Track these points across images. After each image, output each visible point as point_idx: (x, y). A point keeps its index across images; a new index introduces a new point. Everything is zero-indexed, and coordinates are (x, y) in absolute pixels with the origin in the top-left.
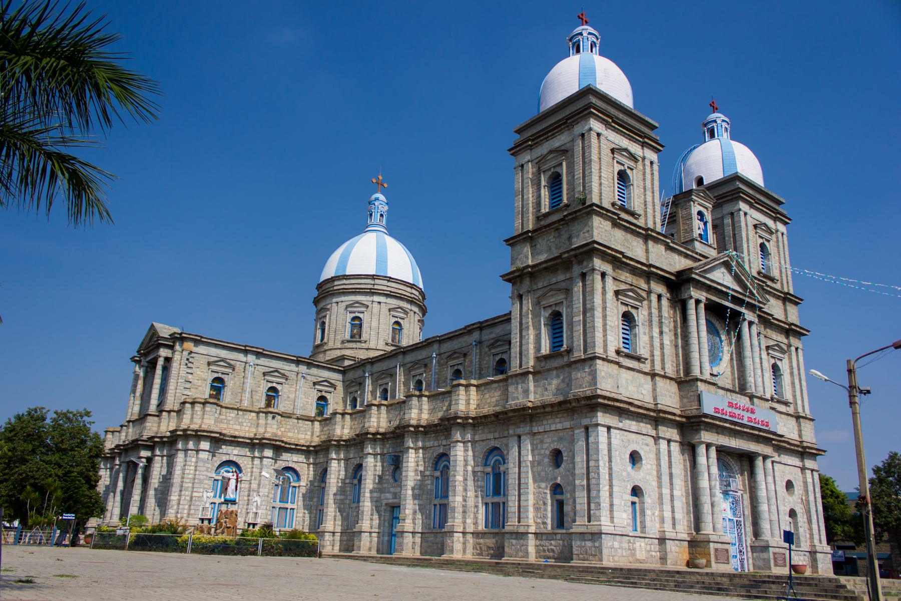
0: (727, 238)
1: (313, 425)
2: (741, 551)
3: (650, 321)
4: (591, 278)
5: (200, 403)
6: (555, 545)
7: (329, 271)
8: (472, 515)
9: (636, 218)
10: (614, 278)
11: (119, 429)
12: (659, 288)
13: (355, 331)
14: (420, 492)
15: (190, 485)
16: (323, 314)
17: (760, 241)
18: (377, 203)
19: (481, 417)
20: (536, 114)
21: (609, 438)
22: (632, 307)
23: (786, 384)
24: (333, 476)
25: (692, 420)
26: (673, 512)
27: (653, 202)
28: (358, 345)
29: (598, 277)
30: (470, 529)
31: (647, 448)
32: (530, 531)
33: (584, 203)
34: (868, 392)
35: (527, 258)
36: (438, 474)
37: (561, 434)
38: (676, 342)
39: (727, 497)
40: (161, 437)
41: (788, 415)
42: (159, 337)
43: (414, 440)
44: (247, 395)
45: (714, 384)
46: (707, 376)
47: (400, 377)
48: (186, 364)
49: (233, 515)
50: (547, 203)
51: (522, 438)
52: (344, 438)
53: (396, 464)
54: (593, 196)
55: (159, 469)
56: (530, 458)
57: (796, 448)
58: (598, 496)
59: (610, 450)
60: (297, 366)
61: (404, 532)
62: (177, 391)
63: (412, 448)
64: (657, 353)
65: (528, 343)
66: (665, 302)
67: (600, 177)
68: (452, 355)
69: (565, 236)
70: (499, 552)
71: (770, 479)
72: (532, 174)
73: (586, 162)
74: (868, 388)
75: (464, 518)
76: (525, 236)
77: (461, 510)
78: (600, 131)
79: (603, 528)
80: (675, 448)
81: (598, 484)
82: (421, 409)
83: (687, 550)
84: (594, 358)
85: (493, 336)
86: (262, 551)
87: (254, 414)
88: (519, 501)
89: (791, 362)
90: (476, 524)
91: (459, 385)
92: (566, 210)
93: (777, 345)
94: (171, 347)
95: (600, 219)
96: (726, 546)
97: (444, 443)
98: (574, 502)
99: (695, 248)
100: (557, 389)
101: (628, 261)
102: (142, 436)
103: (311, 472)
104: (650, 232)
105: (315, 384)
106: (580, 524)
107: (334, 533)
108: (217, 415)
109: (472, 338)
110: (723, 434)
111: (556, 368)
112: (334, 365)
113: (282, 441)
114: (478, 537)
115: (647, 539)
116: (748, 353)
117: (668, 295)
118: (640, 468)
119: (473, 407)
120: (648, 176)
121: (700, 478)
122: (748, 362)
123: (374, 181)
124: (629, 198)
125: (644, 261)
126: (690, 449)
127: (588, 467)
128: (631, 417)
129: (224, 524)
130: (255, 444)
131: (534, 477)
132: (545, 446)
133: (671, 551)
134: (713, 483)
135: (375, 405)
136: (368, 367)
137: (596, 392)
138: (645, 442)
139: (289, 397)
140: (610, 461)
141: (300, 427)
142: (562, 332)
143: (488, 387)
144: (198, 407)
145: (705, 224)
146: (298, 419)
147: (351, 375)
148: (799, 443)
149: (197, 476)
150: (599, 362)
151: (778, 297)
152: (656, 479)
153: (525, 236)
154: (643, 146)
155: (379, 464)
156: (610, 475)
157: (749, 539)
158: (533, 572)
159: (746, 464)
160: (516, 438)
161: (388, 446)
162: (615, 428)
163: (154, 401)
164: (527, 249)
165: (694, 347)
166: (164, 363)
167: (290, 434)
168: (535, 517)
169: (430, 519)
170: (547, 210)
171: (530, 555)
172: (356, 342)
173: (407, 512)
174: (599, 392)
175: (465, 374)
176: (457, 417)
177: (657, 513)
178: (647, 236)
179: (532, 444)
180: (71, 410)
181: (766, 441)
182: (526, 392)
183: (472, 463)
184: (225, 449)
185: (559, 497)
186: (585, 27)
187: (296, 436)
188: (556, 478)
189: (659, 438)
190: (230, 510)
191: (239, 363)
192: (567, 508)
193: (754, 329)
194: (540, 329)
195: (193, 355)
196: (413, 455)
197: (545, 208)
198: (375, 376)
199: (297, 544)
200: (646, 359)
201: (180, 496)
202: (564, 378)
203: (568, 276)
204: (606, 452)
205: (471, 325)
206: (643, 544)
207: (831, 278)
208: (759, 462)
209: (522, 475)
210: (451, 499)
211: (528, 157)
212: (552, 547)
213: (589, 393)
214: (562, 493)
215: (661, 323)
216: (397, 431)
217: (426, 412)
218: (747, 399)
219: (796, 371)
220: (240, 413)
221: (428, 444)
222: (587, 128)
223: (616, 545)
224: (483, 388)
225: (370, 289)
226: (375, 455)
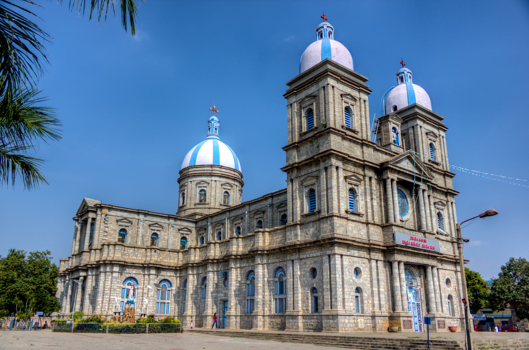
0: (410, 141)
1: (178, 254)
2: (419, 321)
3: (365, 193)
4: (330, 170)
5: (112, 245)
6: (313, 322)
7: (186, 163)
8: (268, 306)
9: (356, 134)
10: (343, 169)
11: (68, 259)
12: (370, 173)
13: (202, 198)
14: (239, 292)
15: (109, 292)
16: (183, 189)
17: (430, 142)
18: (213, 122)
19: (271, 250)
20: (299, 74)
21: (342, 261)
22: (355, 185)
23: (446, 223)
24: (190, 284)
25: (390, 248)
26: (380, 301)
27: (366, 124)
28: (204, 206)
29: (334, 170)
30: (267, 313)
31: (364, 265)
32: (299, 314)
33: (326, 127)
34: (468, 241)
35: (295, 158)
36: (249, 282)
37: (316, 259)
38: (381, 204)
39: (411, 290)
40: (91, 265)
41: (447, 241)
42: (88, 206)
43: (235, 263)
44: (140, 238)
45: (402, 227)
46: (398, 223)
47: (228, 225)
48: (104, 222)
49: (132, 310)
50: (306, 126)
51: (294, 262)
52: (196, 262)
53: (226, 277)
54: (331, 123)
55: (91, 283)
56: (299, 273)
57: (451, 260)
58: (336, 294)
59: (342, 268)
60: (169, 220)
61: (230, 316)
62: (100, 238)
63: (234, 268)
64: (370, 211)
65: (296, 207)
66: (374, 182)
67: (334, 111)
68: (257, 212)
69: (316, 146)
70: (283, 327)
71: (436, 279)
72: (297, 109)
73: (326, 103)
74: (468, 239)
75: (264, 307)
76: (293, 145)
77: (262, 303)
78: (334, 85)
79: (339, 312)
80: (381, 264)
81: (336, 288)
82: (238, 246)
83: (388, 322)
84: (332, 216)
85: (279, 201)
86: (149, 330)
87: (144, 250)
88: (293, 297)
89: (448, 211)
90: (270, 310)
91: (259, 232)
92: (316, 130)
93: (440, 202)
94: (95, 212)
96: (410, 319)
97: (252, 264)
98: (323, 297)
99: (391, 149)
100: (313, 234)
101: (351, 159)
102: (80, 264)
103: (178, 282)
104: (364, 142)
105: (179, 230)
106: (326, 310)
107: (192, 316)
108: (122, 251)
109: (267, 203)
110: (408, 255)
111: (312, 222)
112: (191, 218)
113: (161, 265)
114: (271, 318)
115: (365, 317)
116: (422, 208)
117: (376, 177)
118: (360, 277)
119: (267, 243)
120: (363, 109)
121: (395, 280)
122: (423, 213)
123: (211, 109)
124: (352, 122)
125: (361, 158)
126: (389, 264)
127: (330, 278)
128: (355, 248)
129: (127, 315)
130: (145, 267)
131: (301, 284)
132: (307, 266)
133: (379, 323)
134: (402, 283)
135: (212, 243)
136: (210, 219)
137: (334, 235)
139: (164, 238)
140: (343, 274)
141: (171, 256)
142: (315, 201)
143: (275, 232)
144: (111, 247)
145: (397, 134)
146: (169, 251)
147: (200, 224)
148: (453, 257)
149: (112, 287)
150: (335, 218)
151: (441, 174)
152: (369, 282)
153: (293, 145)
154: (359, 92)
155: (216, 277)
156: (343, 282)
157: (424, 314)
158: (298, 340)
159: (422, 271)
160: (291, 262)
161: (220, 266)
162: (345, 255)
163: (87, 244)
164: (295, 153)
165: (391, 206)
166: (92, 221)
167: (165, 260)
168: (303, 306)
169: (245, 308)
170: (306, 130)
171: (300, 328)
172: (203, 204)
173: (232, 304)
174: (336, 236)
175: (264, 223)
176: (257, 251)
177: (370, 302)
178: (363, 143)
179: (300, 265)
180: (39, 251)
181: (434, 257)
182: (296, 235)
183: (267, 276)
184: (128, 270)
185: (315, 295)
186: (325, 23)
187: (169, 261)
188: (313, 284)
189: (371, 259)
190: (131, 307)
191: (134, 220)
192: (320, 301)
193: (426, 194)
194: (303, 199)
195: (108, 216)
196: (235, 272)
197: (304, 130)
198: (214, 224)
199: (169, 326)
200: (363, 215)
201: (103, 298)
202: (317, 227)
203: (318, 168)
204: (340, 269)
205: (266, 195)
206: (362, 320)
207: (460, 169)
208: (429, 270)
209: (295, 283)
210: (256, 297)
211: (294, 100)
212: (312, 323)
213: (330, 236)
214: (317, 292)
215: (371, 194)
216: (225, 258)
217: (241, 247)
218: (422, 234)
219: (451, 216)
220: (136, 249)
221: (243, 265)
222: (326, 83)
223: (347, 321)
224: (272, 233)
225: (210, 173)
226: (213, 272)
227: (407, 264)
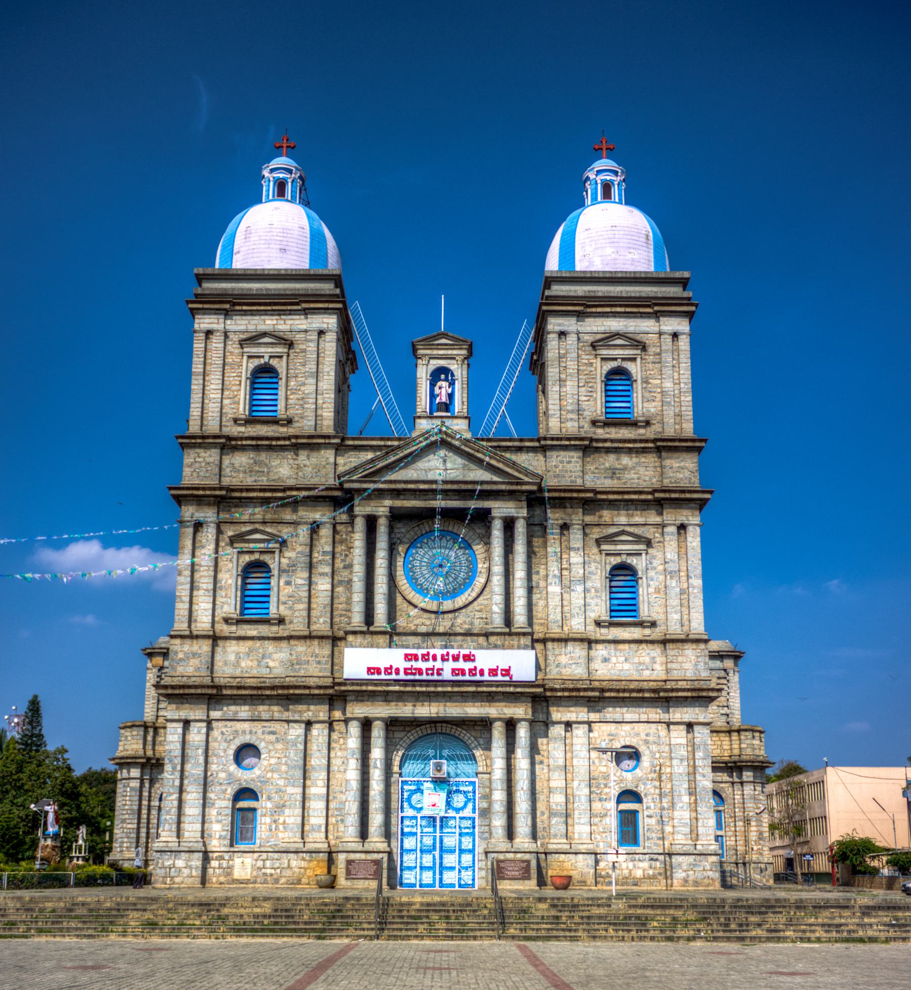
95: (198, 450)
101: (244, 494)
115: (256, 855)
138: (267, 730)
151: (644, 451)
227: (392, 724)
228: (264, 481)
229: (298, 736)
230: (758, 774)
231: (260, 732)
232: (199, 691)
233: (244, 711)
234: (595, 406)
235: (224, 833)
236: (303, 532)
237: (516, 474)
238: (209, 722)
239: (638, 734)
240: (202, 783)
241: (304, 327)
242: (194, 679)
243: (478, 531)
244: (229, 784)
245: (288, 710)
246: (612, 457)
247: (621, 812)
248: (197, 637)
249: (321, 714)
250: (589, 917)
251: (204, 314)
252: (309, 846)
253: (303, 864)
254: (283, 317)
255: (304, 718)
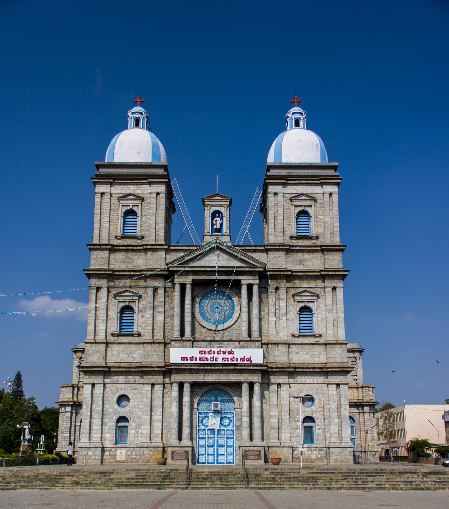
95: (98, 252)
101: (121, 273)
115: (128, 449)
138: (133, 388)
151: (316, 251)
227: (194, 385)
228: (130, 267)
229: (148, 391)
230: (372, 408)
231: (129, 389)
232: (99, 369)
233: (121, 379)
234: (292, 230)
235: (112, 438)
236: (150, 292)
237: (253, 263)
238: (104, 384)
239: (313, 389)
240: (101, 414)
241: (149, 191)
242: (97, 363)
243: (235, 291)
244: (114, 414)
245: (143, 378)
246: (300, 254)
247: (305, 427)
248: (98, 343)
249: (159, 380)
250: (289, 478)
251: (100, 184)
252: (154, 444)
253: (150, 453)
254: (139, 186)
255: (151, 382)
